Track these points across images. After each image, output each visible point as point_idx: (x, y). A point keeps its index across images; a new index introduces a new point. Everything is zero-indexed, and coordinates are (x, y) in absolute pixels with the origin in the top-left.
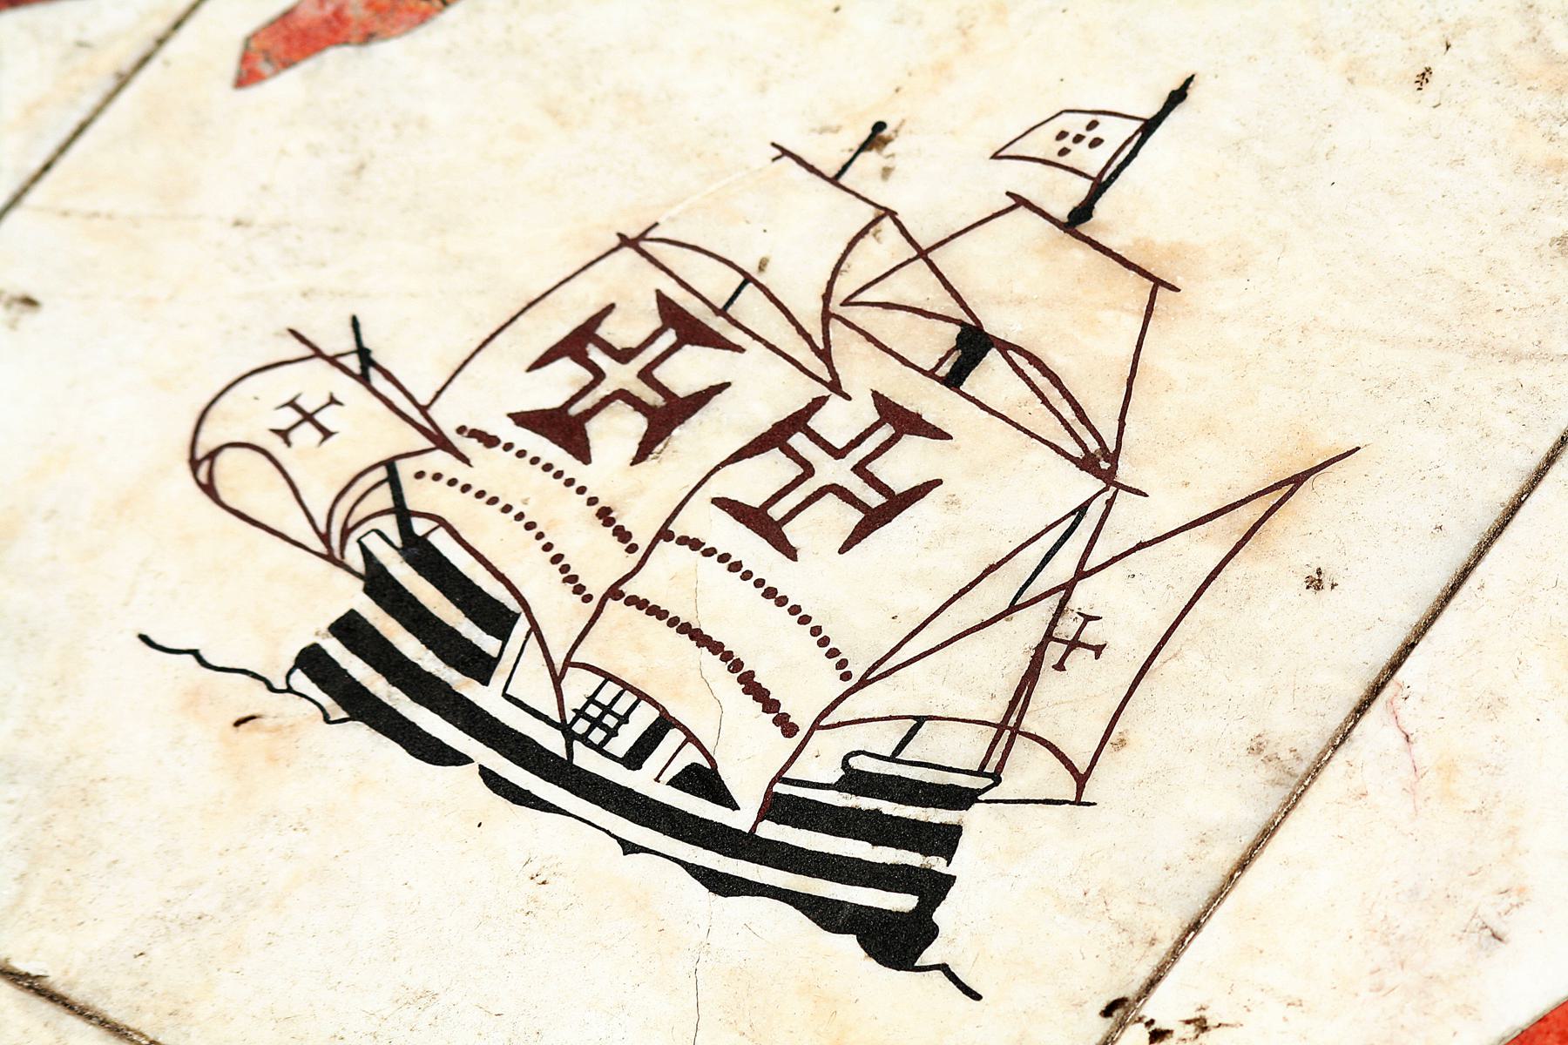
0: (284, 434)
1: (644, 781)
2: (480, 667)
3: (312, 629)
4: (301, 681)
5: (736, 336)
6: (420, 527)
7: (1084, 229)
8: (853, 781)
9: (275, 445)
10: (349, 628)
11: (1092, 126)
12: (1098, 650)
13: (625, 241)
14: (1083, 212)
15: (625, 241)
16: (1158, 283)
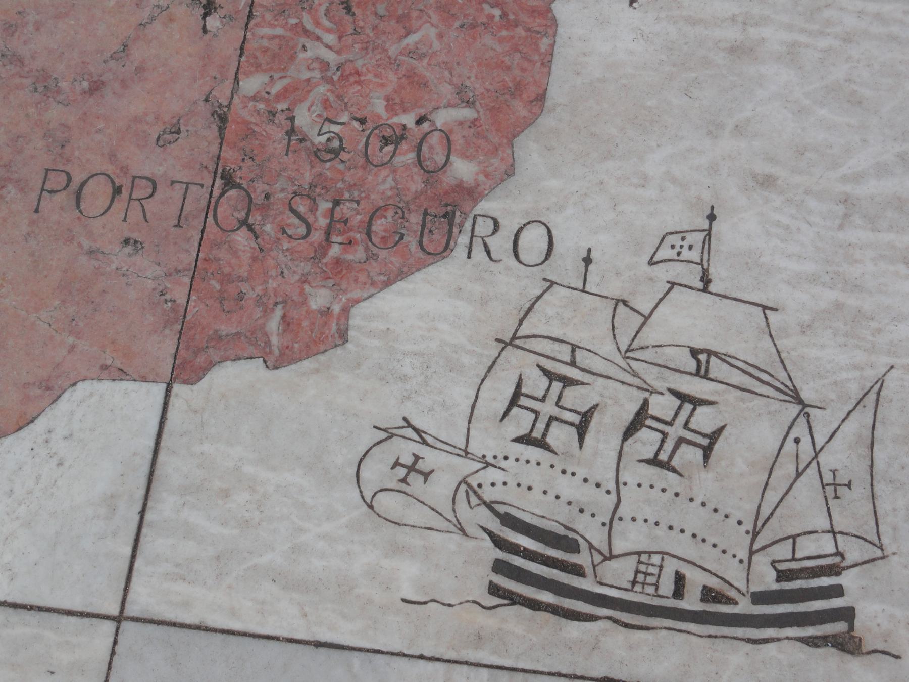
0: (404, 481)
1: (691, 602)
2: (577, 571)
3: (485, 575)
4: (496, 601)
5: (586, 378)
6: (502, 509)
7: (712, 288)
8: (782, 576)
9: (403, 487)
10: (499, 567)
11: (683, 239)
12: (849, 485)
13: (506, 344)
14: (706, 280)
15: (506, 344)
16: (765, 308)
